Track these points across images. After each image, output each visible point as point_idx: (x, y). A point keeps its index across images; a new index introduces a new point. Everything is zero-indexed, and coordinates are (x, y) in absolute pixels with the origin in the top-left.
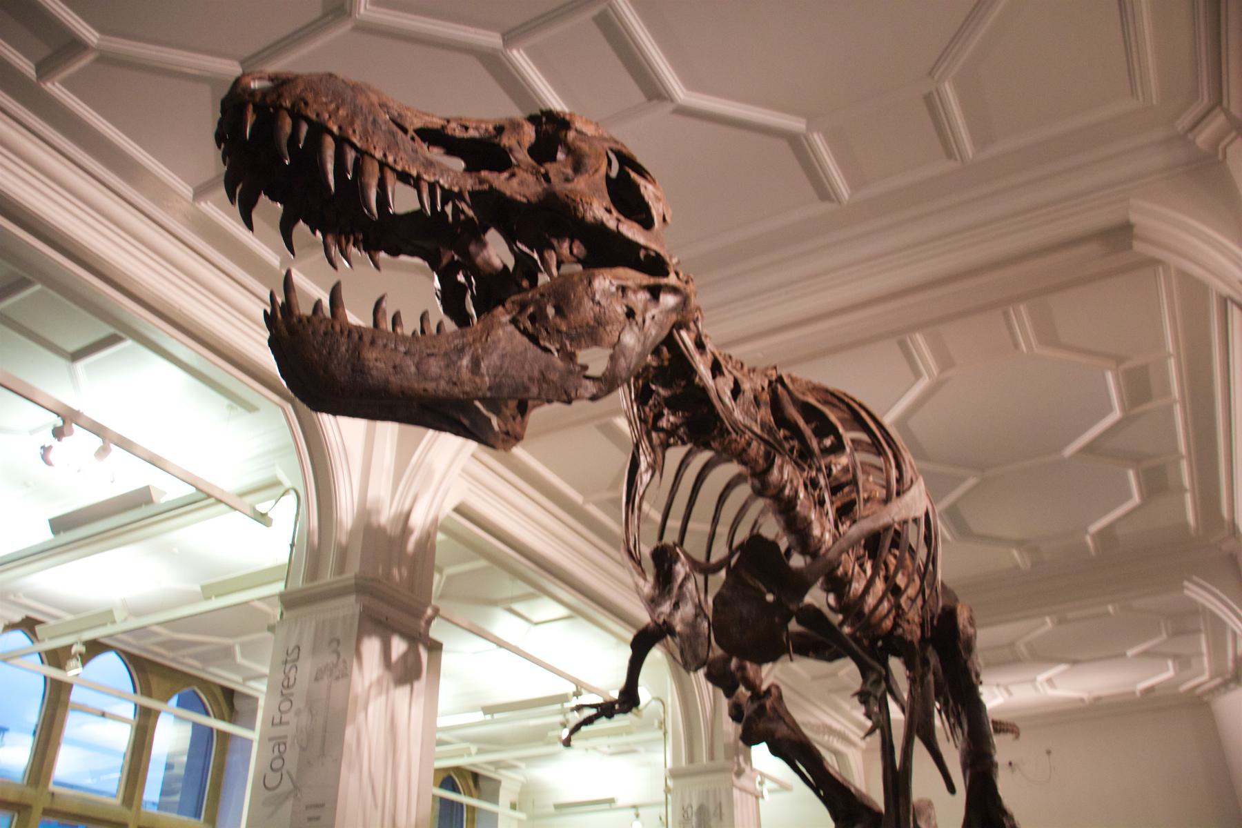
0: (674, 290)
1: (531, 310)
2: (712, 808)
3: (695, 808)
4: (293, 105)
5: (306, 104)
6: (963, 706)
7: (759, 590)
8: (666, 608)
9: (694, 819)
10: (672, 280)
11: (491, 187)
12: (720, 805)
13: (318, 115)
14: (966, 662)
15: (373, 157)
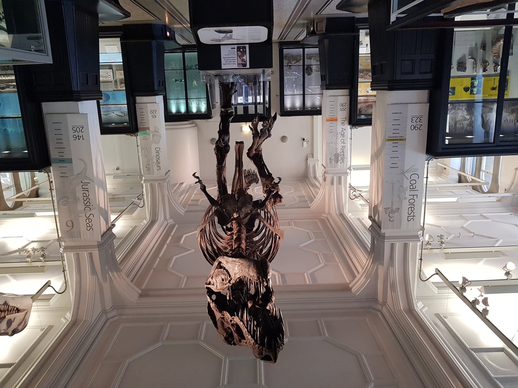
0: (206, 284)
1: (227, 281)
2: (333, 161)
3: (339, 162)
4: (256, 345)
5: (253, 344)
6: (223, 182)
7: (226, 212)
8: (254, 212)
9: (340, 159)
10: (206, 286)
11: (231, 317)
12: (330, 163)
13: (252, 340)
14: (219, 194)
15: (245, 327)
